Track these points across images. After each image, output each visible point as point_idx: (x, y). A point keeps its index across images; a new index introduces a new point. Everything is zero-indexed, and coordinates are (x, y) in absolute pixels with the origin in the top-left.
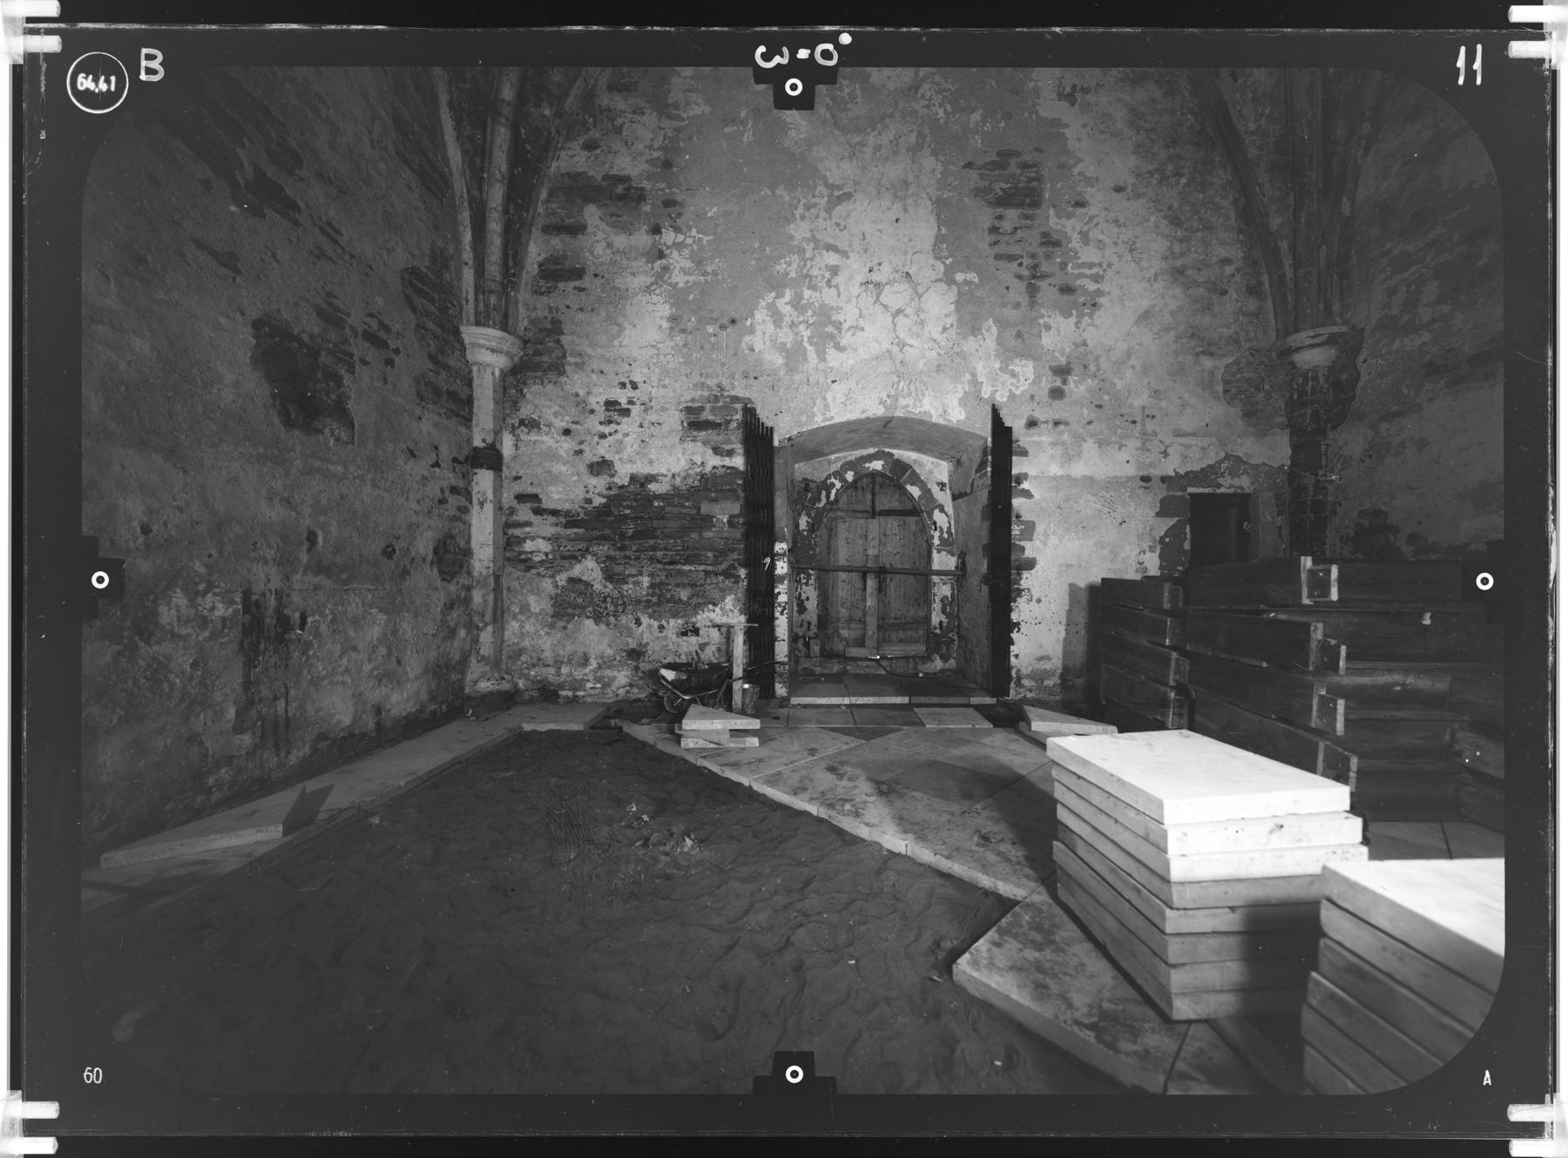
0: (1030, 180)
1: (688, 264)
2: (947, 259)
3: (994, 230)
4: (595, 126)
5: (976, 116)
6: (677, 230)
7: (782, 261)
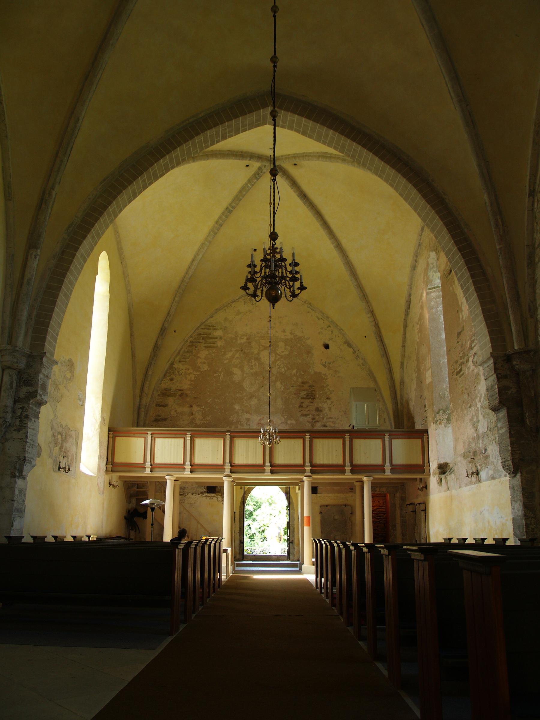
0: (312, 391)
1: (201, 417)
2: (285, 416)
3: (301, 406)
4: (173, 374)
5: (294, 371)
6: (198, 406)
7: (232, 416)
